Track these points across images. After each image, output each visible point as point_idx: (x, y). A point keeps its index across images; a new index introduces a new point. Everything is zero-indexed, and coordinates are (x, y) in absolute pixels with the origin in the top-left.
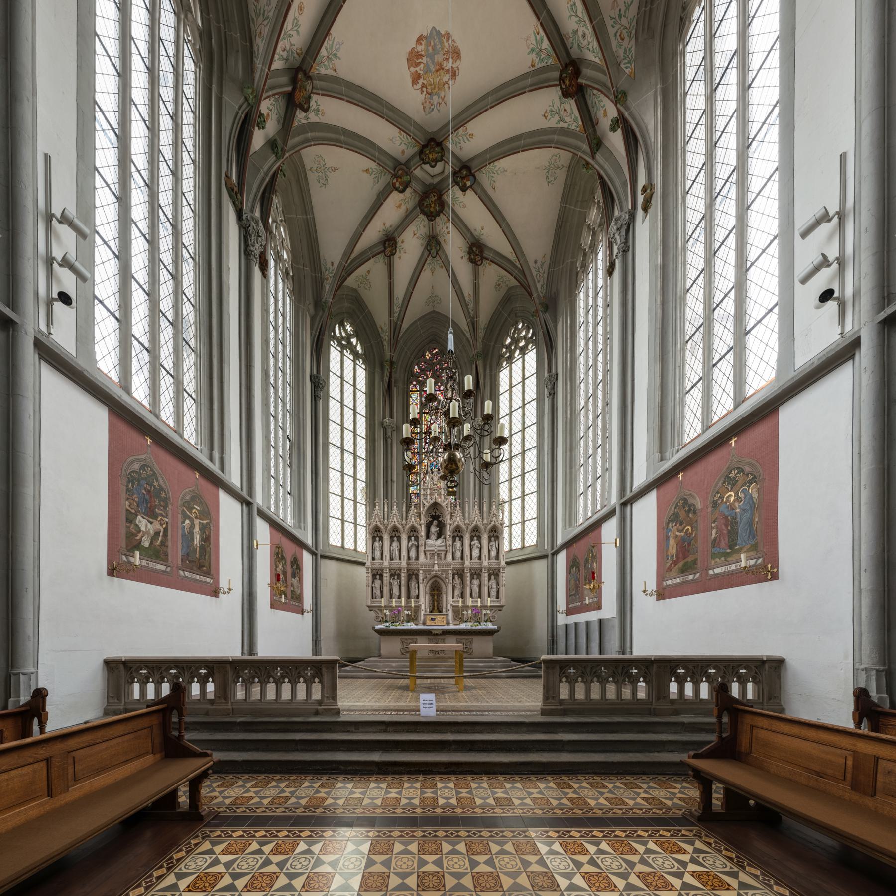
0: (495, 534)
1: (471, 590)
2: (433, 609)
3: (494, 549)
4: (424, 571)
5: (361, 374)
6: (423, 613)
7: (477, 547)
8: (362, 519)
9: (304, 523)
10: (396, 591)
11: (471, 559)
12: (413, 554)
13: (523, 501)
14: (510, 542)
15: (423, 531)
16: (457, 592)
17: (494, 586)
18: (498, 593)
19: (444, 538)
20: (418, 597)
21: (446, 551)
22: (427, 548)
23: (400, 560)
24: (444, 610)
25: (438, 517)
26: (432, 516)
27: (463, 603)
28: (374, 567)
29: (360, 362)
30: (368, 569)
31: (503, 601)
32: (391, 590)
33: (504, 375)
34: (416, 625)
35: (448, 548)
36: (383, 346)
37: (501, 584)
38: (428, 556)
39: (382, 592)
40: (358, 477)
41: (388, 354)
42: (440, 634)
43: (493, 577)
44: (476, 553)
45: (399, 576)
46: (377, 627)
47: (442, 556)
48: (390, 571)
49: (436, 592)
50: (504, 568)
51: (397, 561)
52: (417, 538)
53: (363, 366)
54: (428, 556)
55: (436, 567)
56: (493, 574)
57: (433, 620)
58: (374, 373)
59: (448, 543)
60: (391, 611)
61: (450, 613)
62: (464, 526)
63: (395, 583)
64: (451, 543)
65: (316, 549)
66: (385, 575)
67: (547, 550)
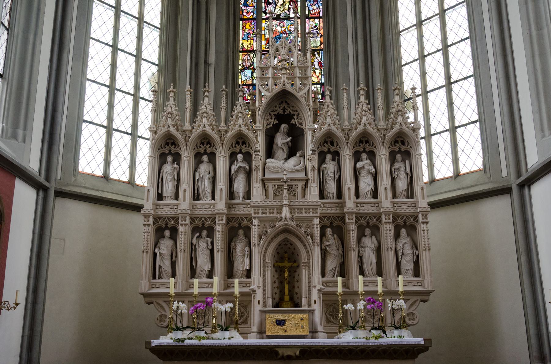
0: (403, 148)
1: (361, 258)
2: (282, 299)
3: (402, 175)
4: (261, 220)
8: (144, 130)
9: (25, 129)
10: (203, 261)
11: (357, 196)
12: (240, 186)
13: (449, 92)
14: (431, 166)
15: (260, 144)
16: (331, 264)
17: (408, 250)
18: (417, 264)
19: (303, 156)
20: (248, 273)
21: (307, 181)
22: (267, 176)
23: (213, 198)
24: (304, 301)
25: (291, 117)
26: (278, 117)
30: (146, 216)
32: (193, 259)
34: (244, 335)
35: (310, 174)
37: (422, 245)
38: (271, 191)
39: (174, 264)
42: (297, 358)
43: (403, 232)
44: (366, 183)
45: (211, 232)
46: (155, 343)
47: (299, 190)
48: (192, 220)
49: (286, 264)
50: (425, 214)
51: (209, 200)
52: (248, 157)
54: (271, 191)
55: (286, 212)
56: (405, 226)
57: (280, 323)
59: (309, 165)
60: (191, 303)
61: (317, 308)
62: (339, 134)
63: (202, 246)
64: (315, 163)
65: (48, 179)
66: (181, 229)
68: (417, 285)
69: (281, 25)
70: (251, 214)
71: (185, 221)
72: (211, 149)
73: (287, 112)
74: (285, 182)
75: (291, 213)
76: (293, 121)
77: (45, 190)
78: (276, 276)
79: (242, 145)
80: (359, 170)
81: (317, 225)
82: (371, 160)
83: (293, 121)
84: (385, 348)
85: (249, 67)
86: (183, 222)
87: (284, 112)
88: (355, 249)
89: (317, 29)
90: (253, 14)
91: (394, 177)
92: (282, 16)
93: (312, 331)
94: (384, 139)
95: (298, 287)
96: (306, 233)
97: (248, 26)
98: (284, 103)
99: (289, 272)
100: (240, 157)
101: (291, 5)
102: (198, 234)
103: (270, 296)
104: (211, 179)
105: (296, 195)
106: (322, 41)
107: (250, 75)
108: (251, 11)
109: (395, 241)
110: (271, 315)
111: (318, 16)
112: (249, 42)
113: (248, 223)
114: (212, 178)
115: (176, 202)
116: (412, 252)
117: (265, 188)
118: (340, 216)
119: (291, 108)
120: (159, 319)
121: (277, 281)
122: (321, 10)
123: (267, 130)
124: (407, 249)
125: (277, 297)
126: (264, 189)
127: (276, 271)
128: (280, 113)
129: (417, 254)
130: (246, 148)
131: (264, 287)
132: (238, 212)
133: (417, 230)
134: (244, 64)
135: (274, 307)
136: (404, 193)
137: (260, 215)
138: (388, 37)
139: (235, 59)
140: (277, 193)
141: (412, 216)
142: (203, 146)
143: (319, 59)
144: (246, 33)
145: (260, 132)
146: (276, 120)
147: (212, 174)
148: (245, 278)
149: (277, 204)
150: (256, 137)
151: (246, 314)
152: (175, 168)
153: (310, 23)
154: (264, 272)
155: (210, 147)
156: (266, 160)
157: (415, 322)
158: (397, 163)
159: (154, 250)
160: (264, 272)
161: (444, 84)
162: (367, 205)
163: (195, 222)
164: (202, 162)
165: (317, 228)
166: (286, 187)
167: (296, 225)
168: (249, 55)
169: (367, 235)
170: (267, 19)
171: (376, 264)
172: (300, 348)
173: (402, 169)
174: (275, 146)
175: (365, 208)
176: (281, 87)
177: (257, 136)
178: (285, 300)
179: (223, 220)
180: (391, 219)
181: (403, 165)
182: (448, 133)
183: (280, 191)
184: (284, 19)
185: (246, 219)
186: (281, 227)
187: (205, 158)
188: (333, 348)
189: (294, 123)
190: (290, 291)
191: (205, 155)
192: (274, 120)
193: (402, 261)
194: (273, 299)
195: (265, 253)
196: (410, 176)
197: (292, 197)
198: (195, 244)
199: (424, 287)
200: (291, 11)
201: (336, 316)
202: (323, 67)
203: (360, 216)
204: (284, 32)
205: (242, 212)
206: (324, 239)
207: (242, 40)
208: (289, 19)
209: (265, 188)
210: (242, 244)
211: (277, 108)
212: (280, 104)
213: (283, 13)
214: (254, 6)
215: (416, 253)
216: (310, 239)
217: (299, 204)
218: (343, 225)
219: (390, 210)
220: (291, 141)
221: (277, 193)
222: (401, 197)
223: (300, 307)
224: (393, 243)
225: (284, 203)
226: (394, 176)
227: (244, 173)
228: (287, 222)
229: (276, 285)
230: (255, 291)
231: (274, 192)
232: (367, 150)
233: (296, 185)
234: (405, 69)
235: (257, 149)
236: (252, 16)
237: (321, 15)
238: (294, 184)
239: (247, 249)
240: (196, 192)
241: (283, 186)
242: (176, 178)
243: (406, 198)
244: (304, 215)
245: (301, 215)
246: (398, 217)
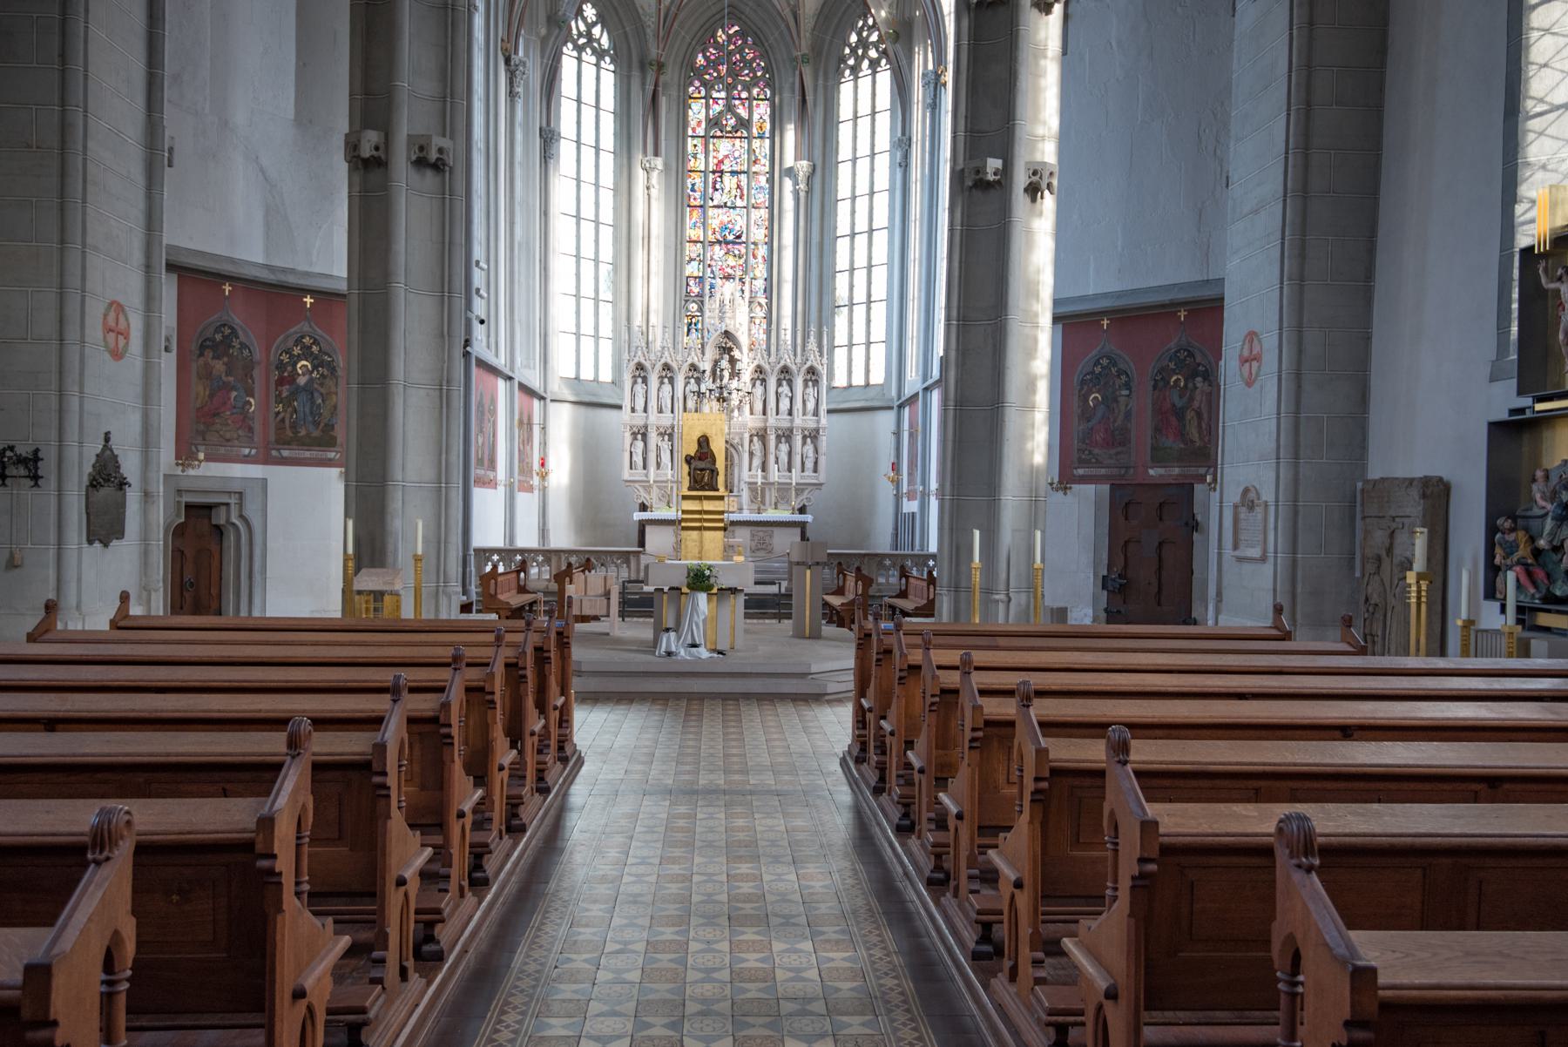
5: (608, 79)
7: (787, 396)
11: (777, 414)
16: (757, 462)
17: (811, 454)
18: (816, 463)
23: (672, 412)
24: (735, 489)
25: (730, 349)
27: (765, 477)
28: (634, 422)
29: (607, 64)
31: (822, 477)
32: (658, 456)
33: (846, 89)
36: (645, 35)
39: (645, 460)
41: (654, 52)
43: (809, 440)
44: (785, 404)
53: (612, 67)
56: (810, 436)
58: (629, 77)
67: (892, 400)
77: (542, 398)
92: (729, 204)
97: (695, 213)
100: (692, 381)
138: (826, 241)
139: (682, 250)
153: (755, 214)
170: (714, 207)
184: (730, 208)
187: (666, 380)
200: (738, 198)
204: (729, 222)
208: (734, 208)
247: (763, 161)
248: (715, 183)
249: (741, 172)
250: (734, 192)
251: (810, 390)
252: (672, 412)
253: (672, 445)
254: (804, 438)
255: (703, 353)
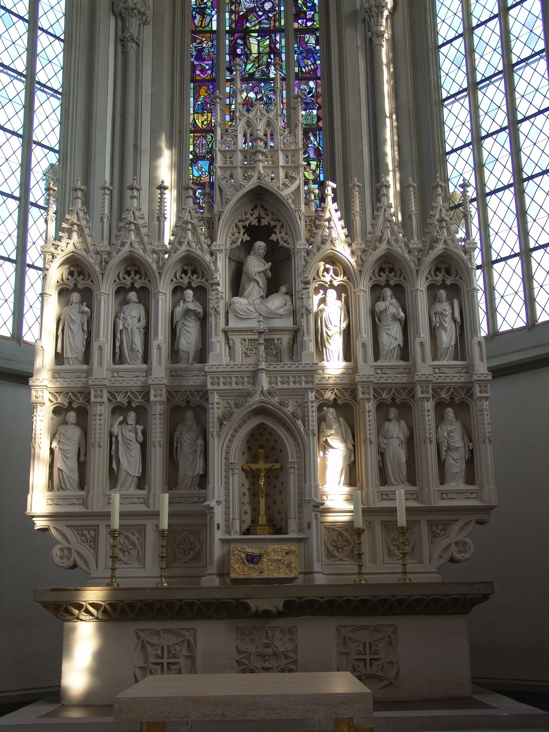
2: (254, 521)
4: (222, 394)
6: (218, 535)
7: (395, 318)
11: (377, 357)
13: (520, 195)
14: (492, 311)
17: (458, 441)
18: (470, 462)
22: (233, 324)
26: (250, 230)
32: (113, 457)
40: (38, 135)
42: (280, 614)
43: (450, 412)
49: (262, 465)
56: (452, 403)
68: (470, 498)
69: (256, 90)
70: (207, 386)
71: (101, 397)
72: (142, 281)
73: (264, 222)
74: (260, 333)
75: (270, 383)
76: (274, 237)
78: (247, 485)
79: (193, 275)
80: (379, 315)
81: (312, 402)
82: (398, 299)
83: (274, 237)
84: (420, 597)
85: (205, 156)
86: (99, 400)
87: (259, 222)
88: (372, 441)
89: (312, 97)
90: (212, 73)
91: (435, 327)
93: (304, 571)
94: (419, 265)
95: (282, 502)
96: (295, 414)
97: (203, 92)
98: (259, 207)
99: (267, 477)
101: (271, 59)
102: (121, 418)
103: (237, 517)
104: (142, 330)
105: (279, 355)
106: (320, 115)
107: (206, 168)
108: (207, 67)
109: (437, 428)
110: (239, 546)
111: (314, 76)
112: (205, 117)
113: (202, 400)
114: (143, 328)
115: (85, 367)
116: (463, 445)
117: (228, 344)
118: (349, 389)
119: (270, 216)
120: (58, 554)
121: (247, 494)
122: (319, 66)
123: (232, 250)
124: (456, 440)
125: (248, 519)
126: (227, 345)
127: (247, 477)
128: (253, 223)
129: (470, 448)
130: (199, 280)
131: (227, 502)
132: (184, 383)
133: (471, 411)
134: (197, 151)
135: (244, 534)
136: (451, 351)
137: (222, 387)
140: (249, 352)
141: (462, 388)
142: (129, 276)
143: (315, 143)
144: (200, 103)
145: (221, 255)
146: (246, 235)
147: (143, 322)
148: (197, 488)
149: (247, 369)
150: (213, 262)
151: (199, 546)
152: (83, 312)
154: (227, 478)
155: (140, 278)
156: (230, 299)
157: (467, 556)
158: (439, 304)
159: (51, 444)
160: (227, 478)
161: (512, 181)
162: (392, 370)
163: (116, 399)
164: (126, 302)
165: (312, 407)
166: (263, 342)
167: (278, 403)
168: (205, 137)
169: (392, 419)
171: (407, 465)
172: (285, 599)
173: (448, 312)
174: (244, 277)
175: (389, 375)
176: (255, 182)
177: (216, 260)
178: (260, 523)
179: (161, 395)
180: (431, 391)
181: (448, 306)
182: (517, 258)
183: (254, 349)
184: (260, 81)
185: (199, 394)
186: (255, 406)
187: (133, 296)
188: (336, 599)
189: (275, 239)
190: (268, 509)
191: (132, 291)
192: (243, 235)
193: (447, 460)
194: (242, 521)
195: (229, 447)
196: (460, 324)
197: (273, 358)
198: (116, 434)
199: (482, 501)
201: (342, 548)
202: (322, 156)
203: (380, 389)
205: (191, 383)
206: (323, 425)
207: (194, 114)
209: (228, 344)
210: (191, 433)
211: (248, 216)
212: (252, 210)
213: (259, 72)
214: (213, 60)
215: (469, 447)
216: (301, 424)
217: (283, 369)
218: (353, 403)
219: (428, 379)
220: (271, 269)
221: (249, 352)
222: (446, 358)
223: (284, 534)
224: (433, 430)
225: (261, 367)
226: (433, 325)
227: (195, 320)
228: (263, 398)
229: (247, 499)
230: (213, 508)
231: (244, 351)
232: (392, 283)
233: (278, 339)
234: (452, 158)
235: (215, 281)
236: (209, 76)
237: (319, 74)
238: (275, 336)
239: (200, 442)
240: (117, 350)
241: (257, 340)
242: (86, 328)
243: (453, 360)
244: (292, 386)
245: (286, 386)
246: (442, 388)
247: (310, 14)
248: (233, 47)
249: (280, 30)
250: (265, 58)
251: (445, 307)
252: (146, 359)
253: (144, 433)
254: (440, 407)
255: (212, 236)
